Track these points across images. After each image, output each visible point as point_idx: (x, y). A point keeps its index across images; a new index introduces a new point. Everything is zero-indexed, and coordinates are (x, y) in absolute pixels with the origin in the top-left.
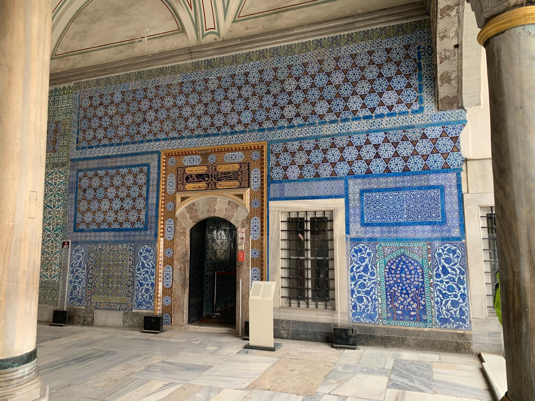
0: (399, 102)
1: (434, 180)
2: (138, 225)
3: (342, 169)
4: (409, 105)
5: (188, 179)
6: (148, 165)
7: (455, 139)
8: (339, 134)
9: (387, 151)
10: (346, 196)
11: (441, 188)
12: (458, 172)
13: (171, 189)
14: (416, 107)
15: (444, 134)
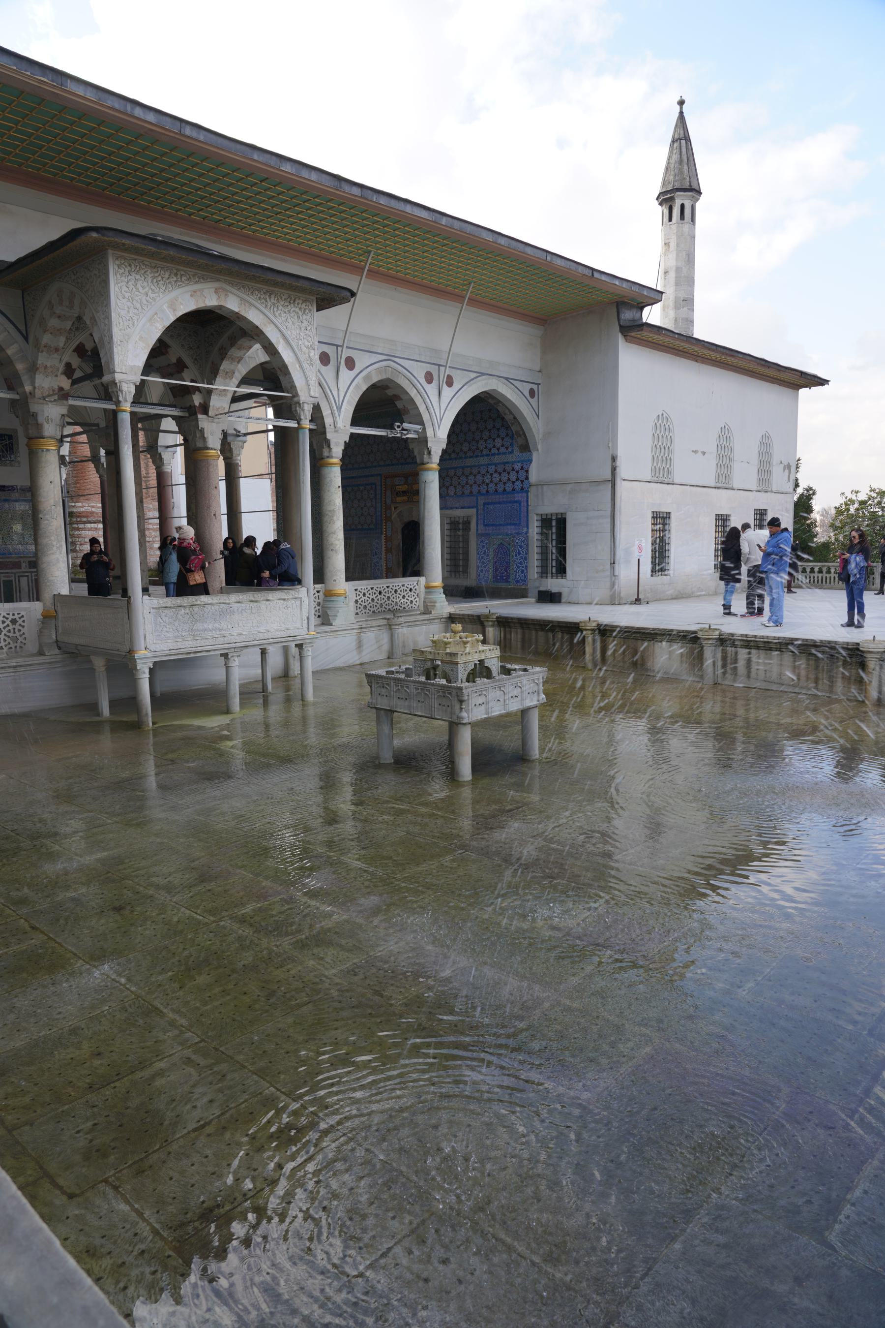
0: (503, 446)
1: (518, 496)
2: (372, 526)
3: (475, 489)
4: (507, 448)
5: (399, 494)
6: (375, 484)
7: (527, 471)
8: (475, 466)
9: (496, 478)
10: (476, 507)
11: (519, 502)
12: (527, 492)
13: (389, 501)
14: (510, 450)
15: (522, 468)
